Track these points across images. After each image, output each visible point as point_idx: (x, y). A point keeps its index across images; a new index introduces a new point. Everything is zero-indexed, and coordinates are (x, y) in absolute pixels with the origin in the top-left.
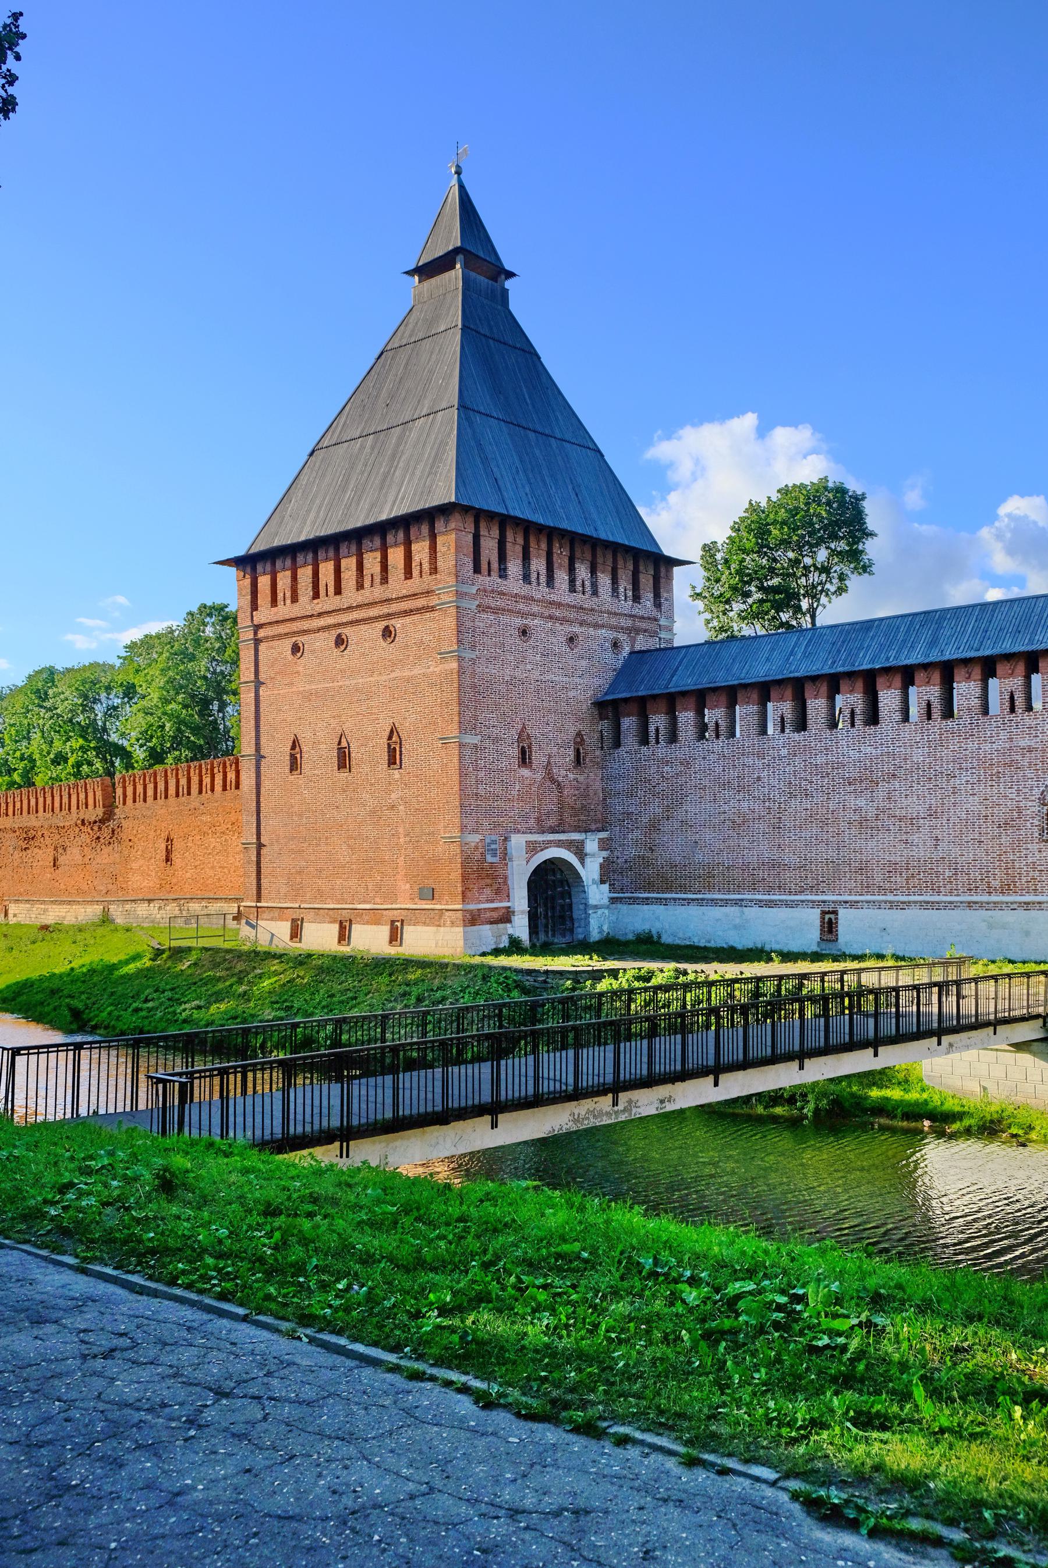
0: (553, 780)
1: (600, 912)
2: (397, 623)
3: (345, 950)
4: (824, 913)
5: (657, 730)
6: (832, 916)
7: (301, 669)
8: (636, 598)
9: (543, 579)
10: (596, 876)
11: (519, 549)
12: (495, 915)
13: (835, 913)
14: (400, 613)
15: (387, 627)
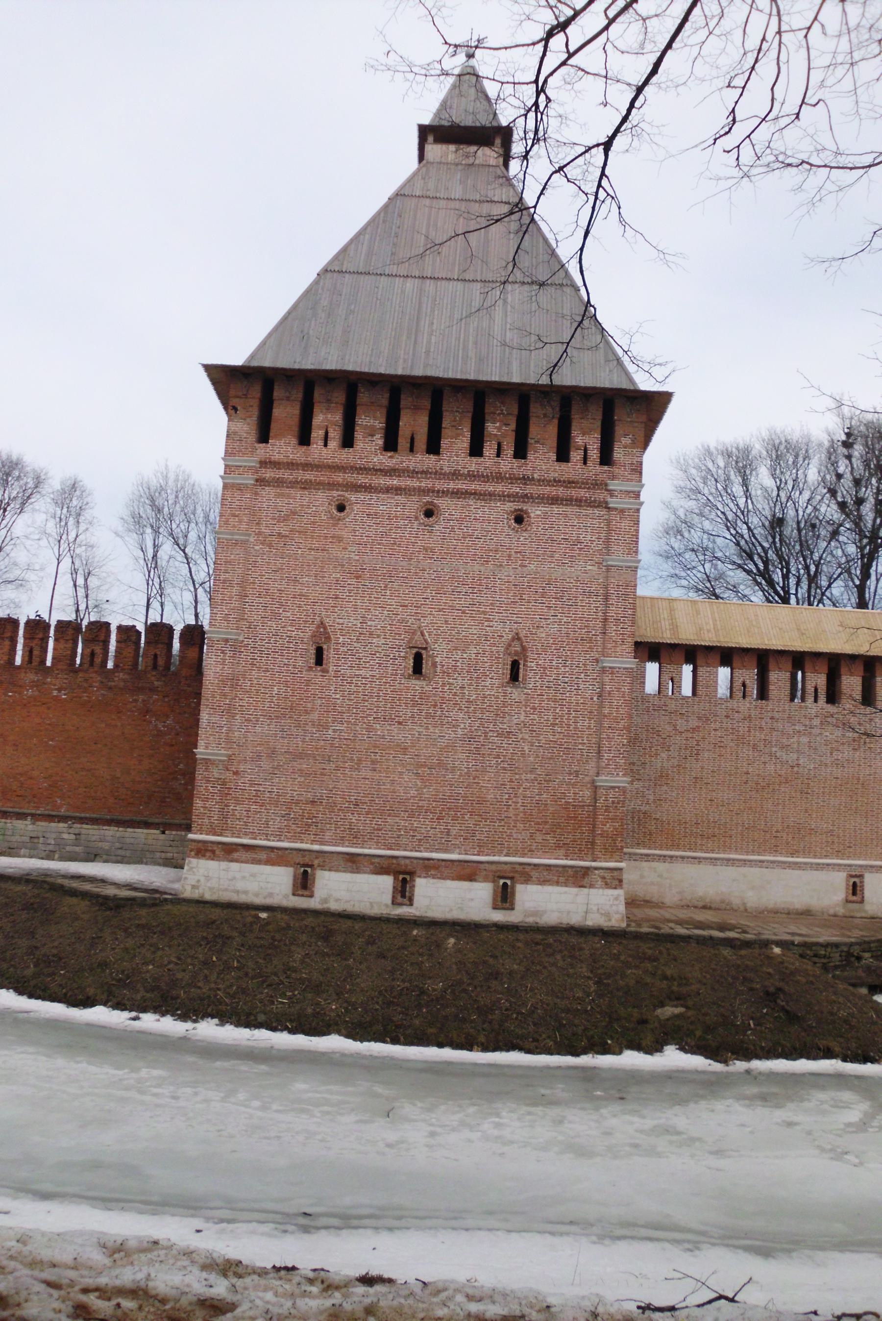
3: (404, 911)
6: (857, 880)
7: (344, 533)
13: (861, 876)
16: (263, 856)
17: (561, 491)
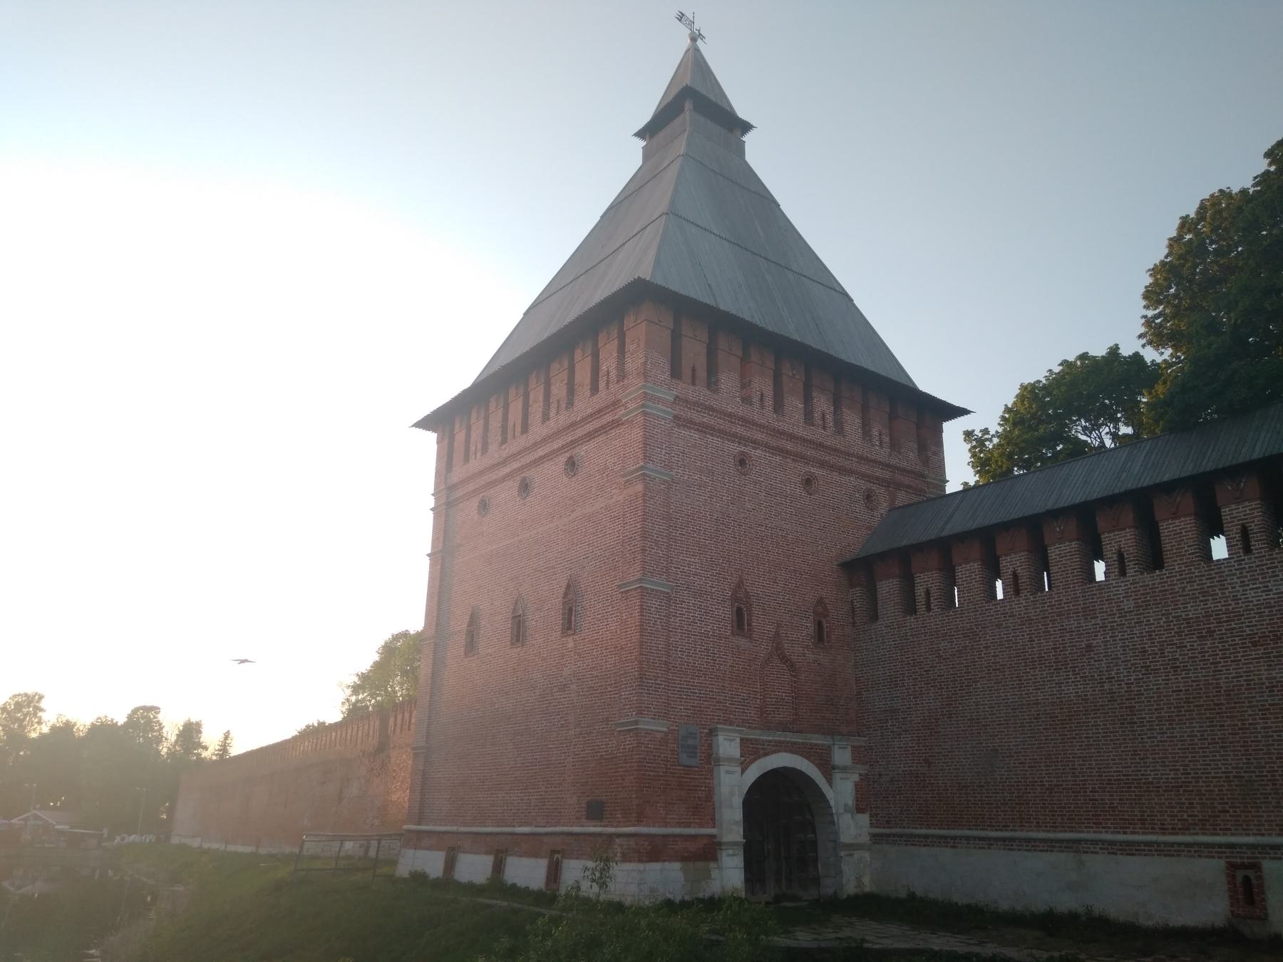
0: (785, 659)
1: (857, 854)
4: (1232, 867)
5: (928, 593)
6: (1250, 873)
9: (769, 402)
10: (850, 801)
13: (1256, 867)
14: (581, 438)
15: (571, 457)
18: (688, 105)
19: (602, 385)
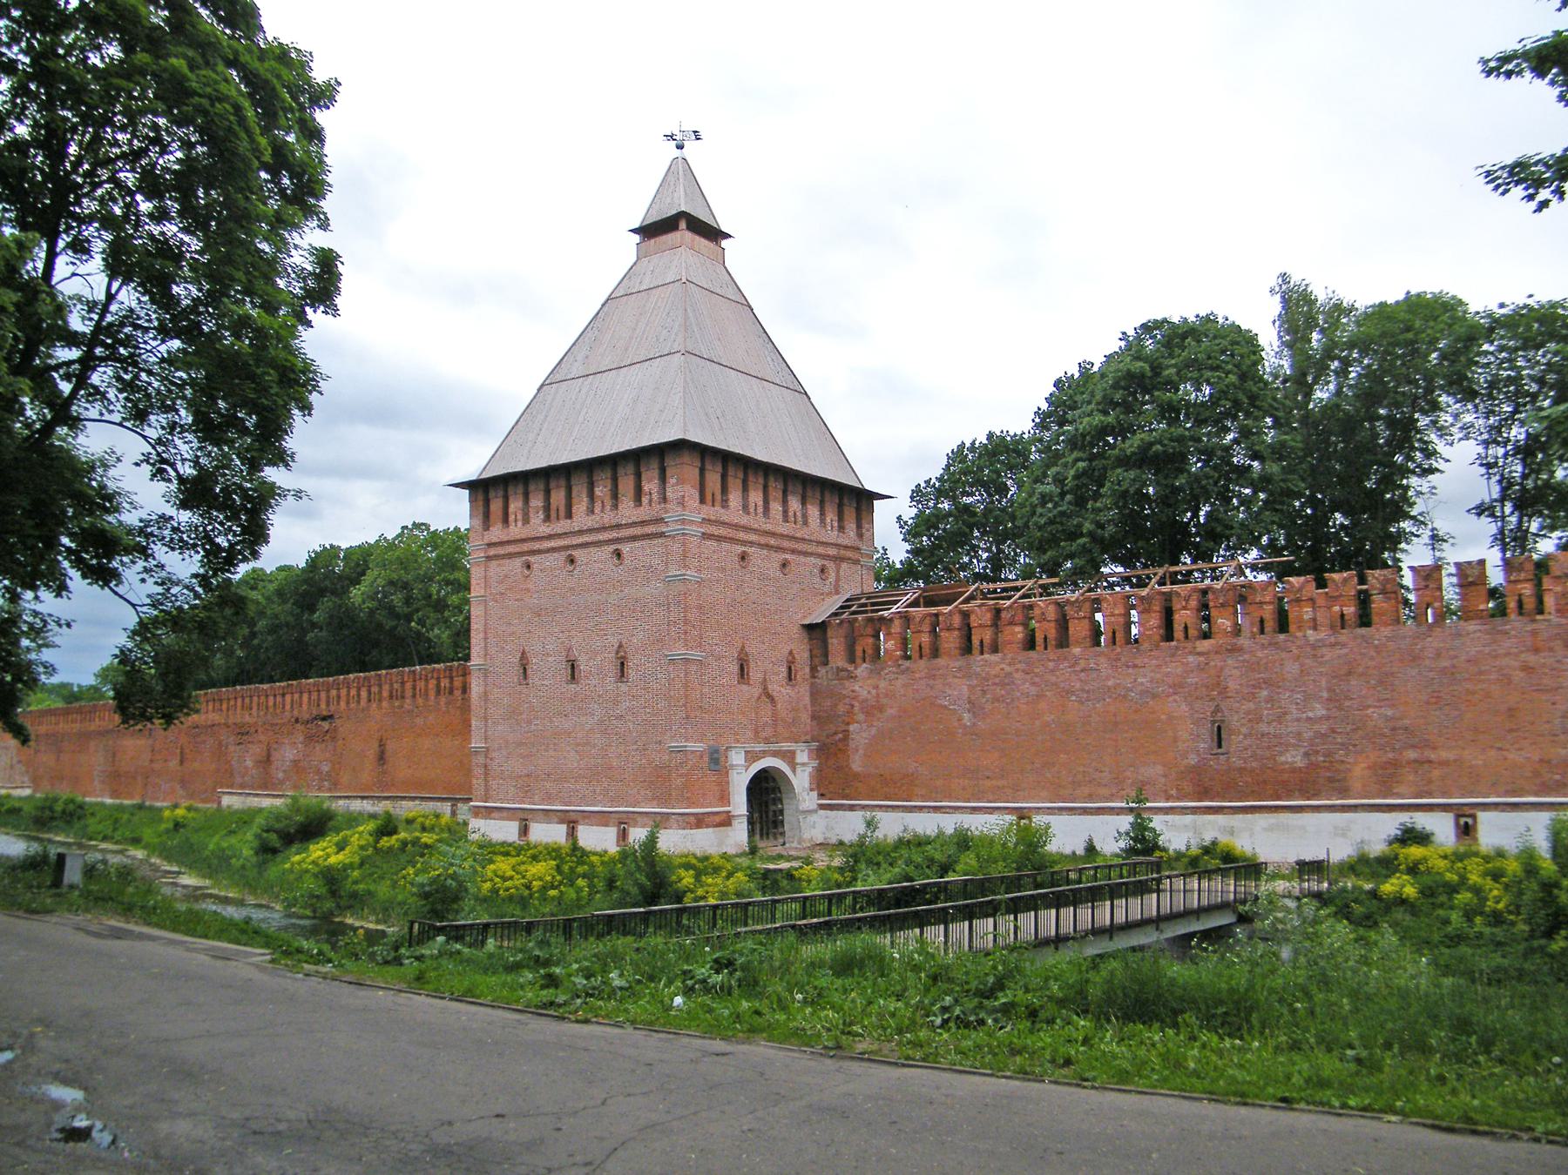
2: (625, 548)
7: (531, 586)
8: (841, 528)
9: (760, 510)
10: (807, 785)
11: (739, 482)
12: (718, 819)
16: (505, 814)
17: (638, 531)
18: (683, 225)
19: (645, 500)
